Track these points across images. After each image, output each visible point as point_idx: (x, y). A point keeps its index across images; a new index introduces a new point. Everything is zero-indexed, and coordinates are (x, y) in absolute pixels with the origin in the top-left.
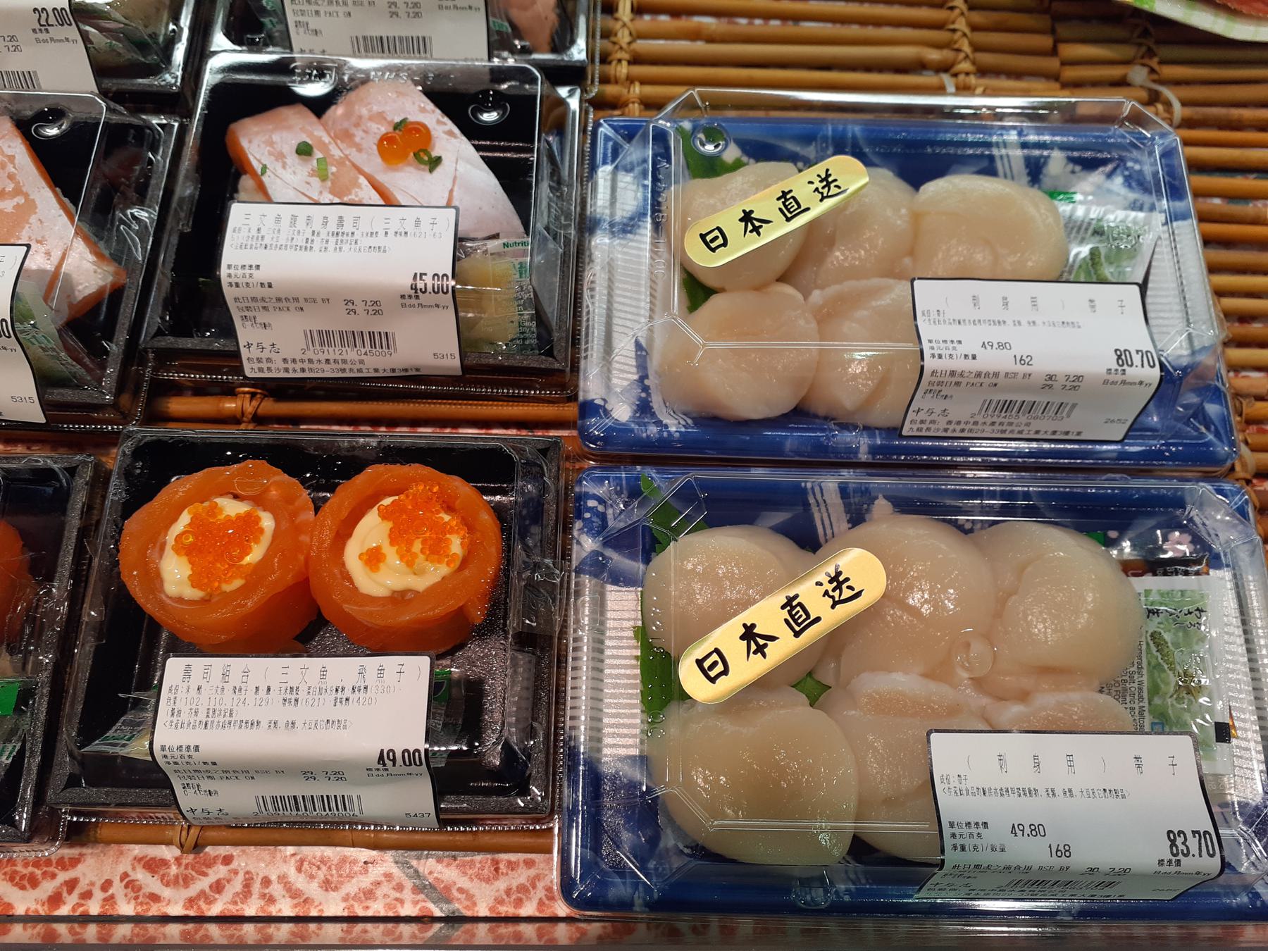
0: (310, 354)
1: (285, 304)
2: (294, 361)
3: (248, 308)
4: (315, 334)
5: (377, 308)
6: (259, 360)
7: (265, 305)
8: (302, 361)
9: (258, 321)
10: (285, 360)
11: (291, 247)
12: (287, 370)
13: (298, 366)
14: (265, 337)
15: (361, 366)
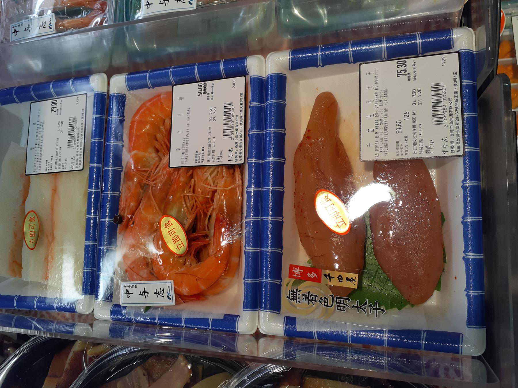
0: (447, 123)
1: (58, 153)
2: (452, 131)
3: (59, 165)
4: (434, 120)
5: (61, 123)
6: (77, 164)
7: (58, 159)
8: (451, 127)
9: (429, 145)
10: (77, 155)
11: (40, 152)
12: (81, 155)
13: (79, 150)
14: (69, 161)
15: (80, 129)
